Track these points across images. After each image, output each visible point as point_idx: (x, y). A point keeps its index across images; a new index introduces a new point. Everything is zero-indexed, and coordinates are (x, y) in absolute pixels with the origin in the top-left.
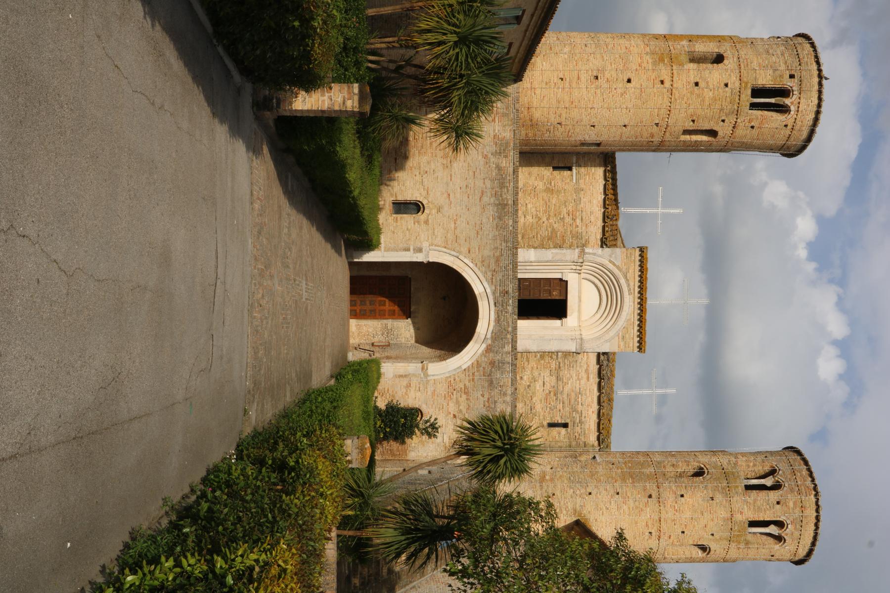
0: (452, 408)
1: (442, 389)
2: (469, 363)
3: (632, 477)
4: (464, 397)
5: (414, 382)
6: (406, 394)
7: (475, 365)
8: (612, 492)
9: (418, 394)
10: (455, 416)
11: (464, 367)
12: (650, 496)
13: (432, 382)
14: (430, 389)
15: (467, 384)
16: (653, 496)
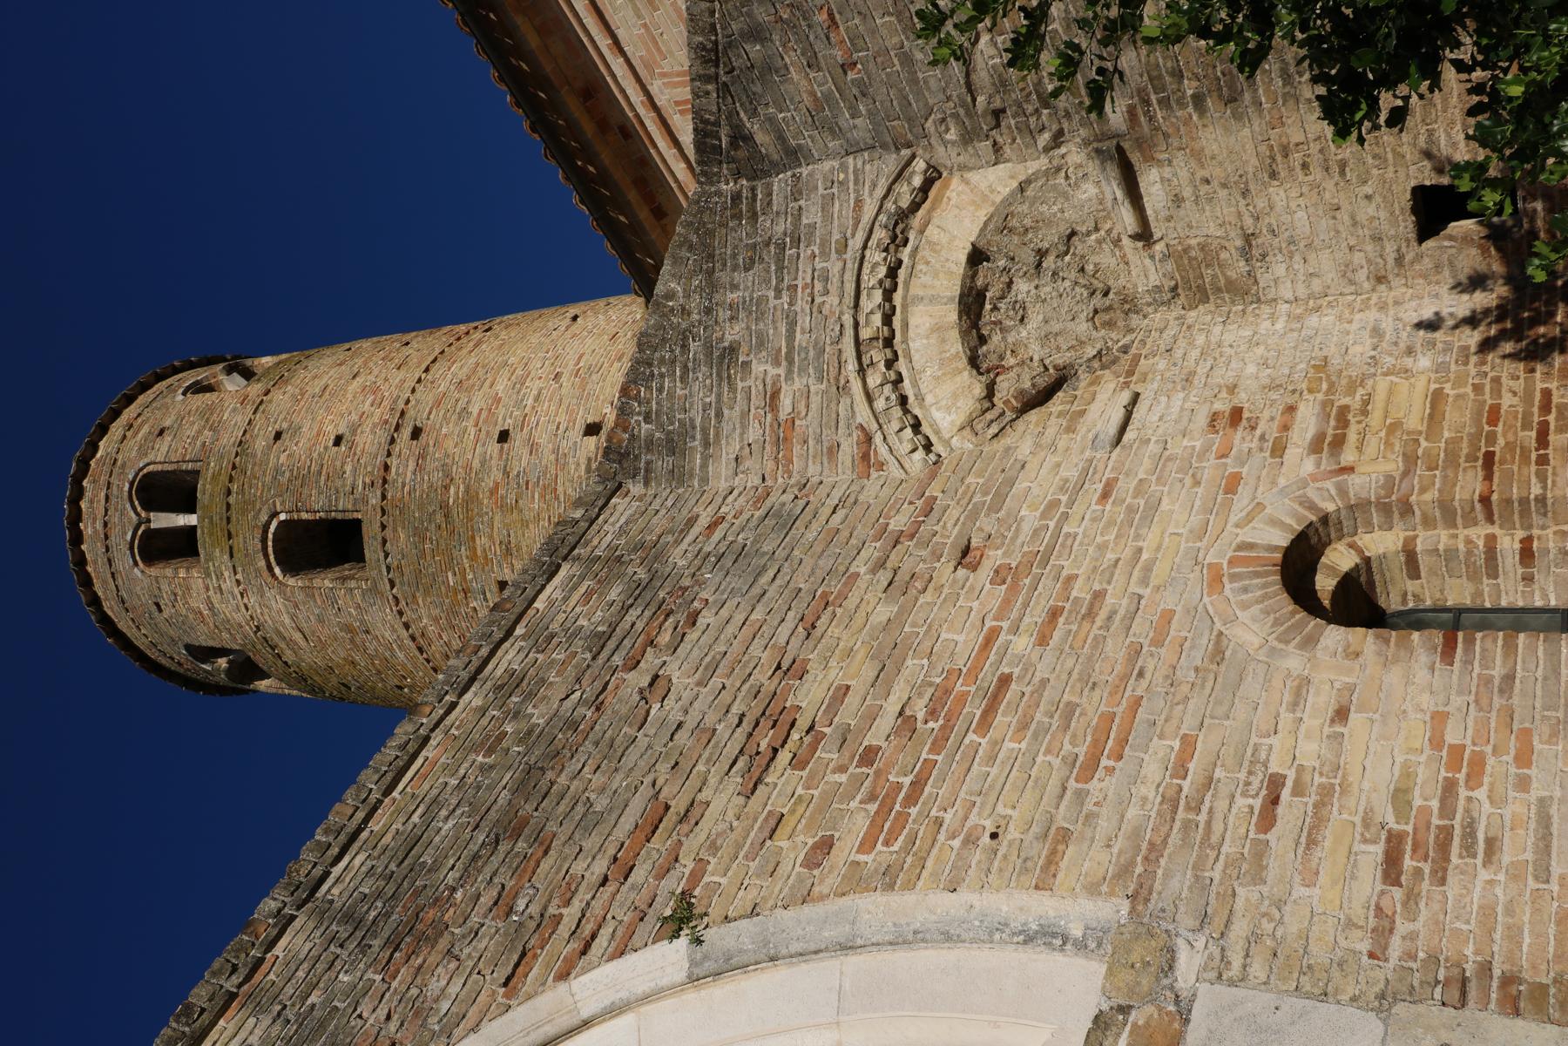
0: (957, 617)
1: (1001, 775)
2: (595, 985)
3: (444, 506)
4: (808, 696)
5: (1333, 892)
6: (1464, 766)
7: (561, 945)
8: (517, 439)
9: (1300, 746)
10: (965, 555)
11: (672, 956)
12: (416, 433)
13: (1090, 857)
14: (1136, 787)
15: (722, 799)
16: (406, 432)
